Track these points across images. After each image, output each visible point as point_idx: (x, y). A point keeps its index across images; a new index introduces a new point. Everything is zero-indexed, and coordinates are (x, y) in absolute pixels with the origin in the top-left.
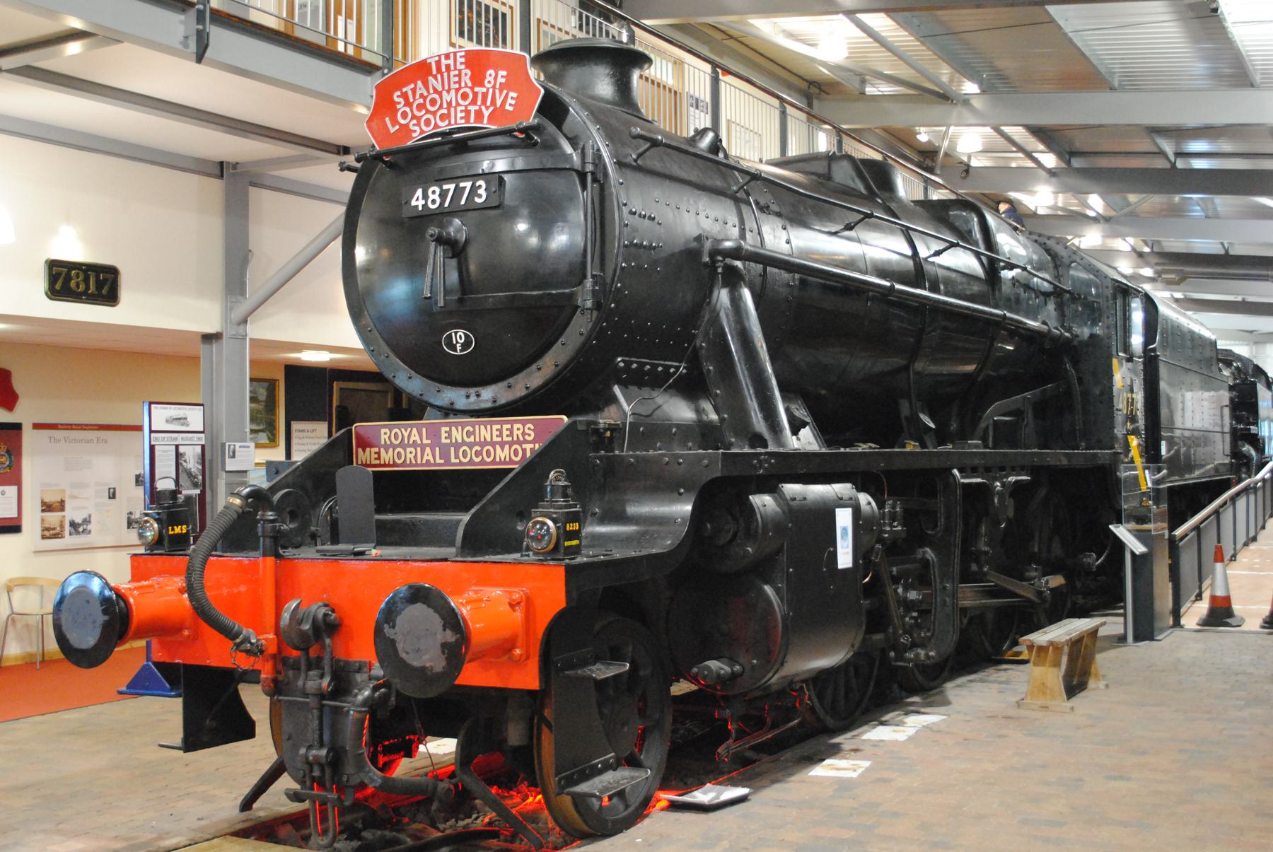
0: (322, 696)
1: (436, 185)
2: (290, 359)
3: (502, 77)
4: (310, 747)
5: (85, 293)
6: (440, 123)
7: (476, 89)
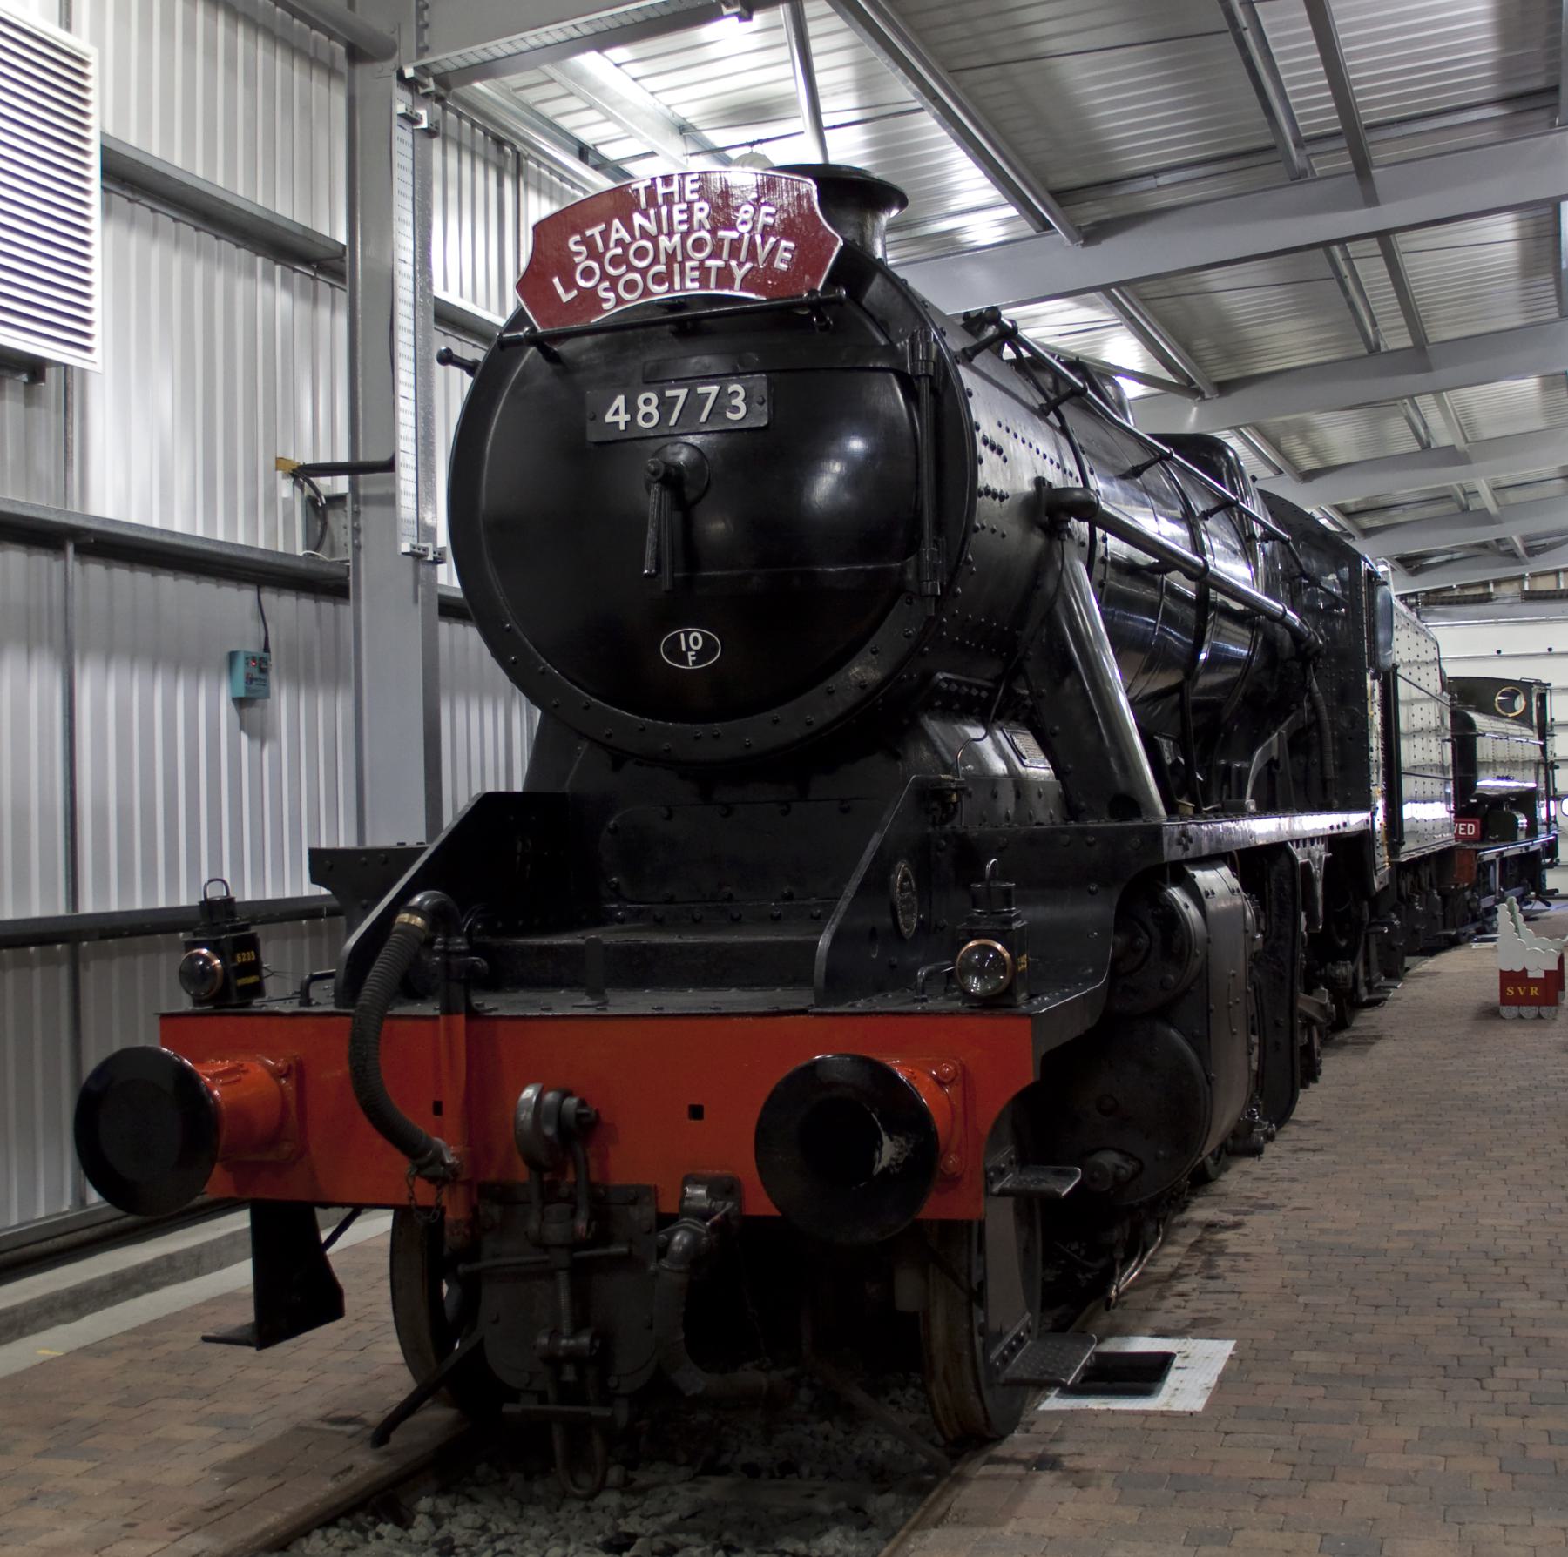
6: (655, 288)
7: (721, 233)
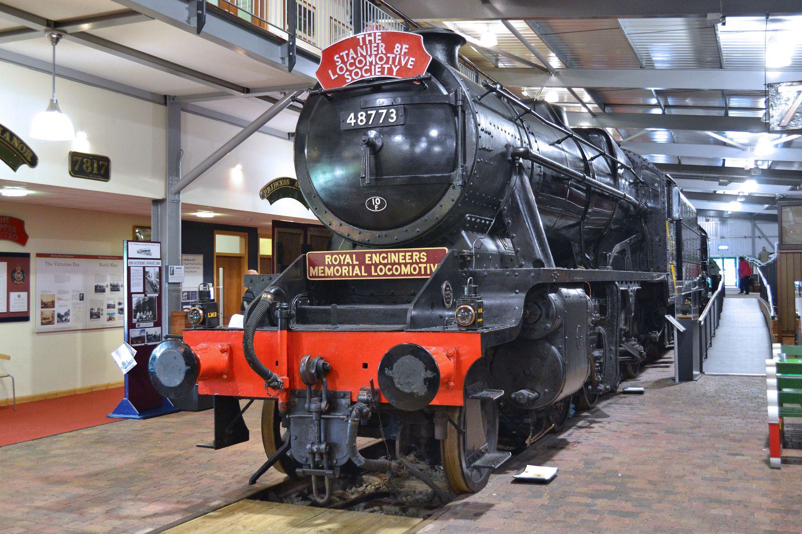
0: (320, 412)
1: (362, 111)
2: (189, 216)
3: (406, 48)
4: (313, 444)
5: (91, 173)
7: (389, 55)
